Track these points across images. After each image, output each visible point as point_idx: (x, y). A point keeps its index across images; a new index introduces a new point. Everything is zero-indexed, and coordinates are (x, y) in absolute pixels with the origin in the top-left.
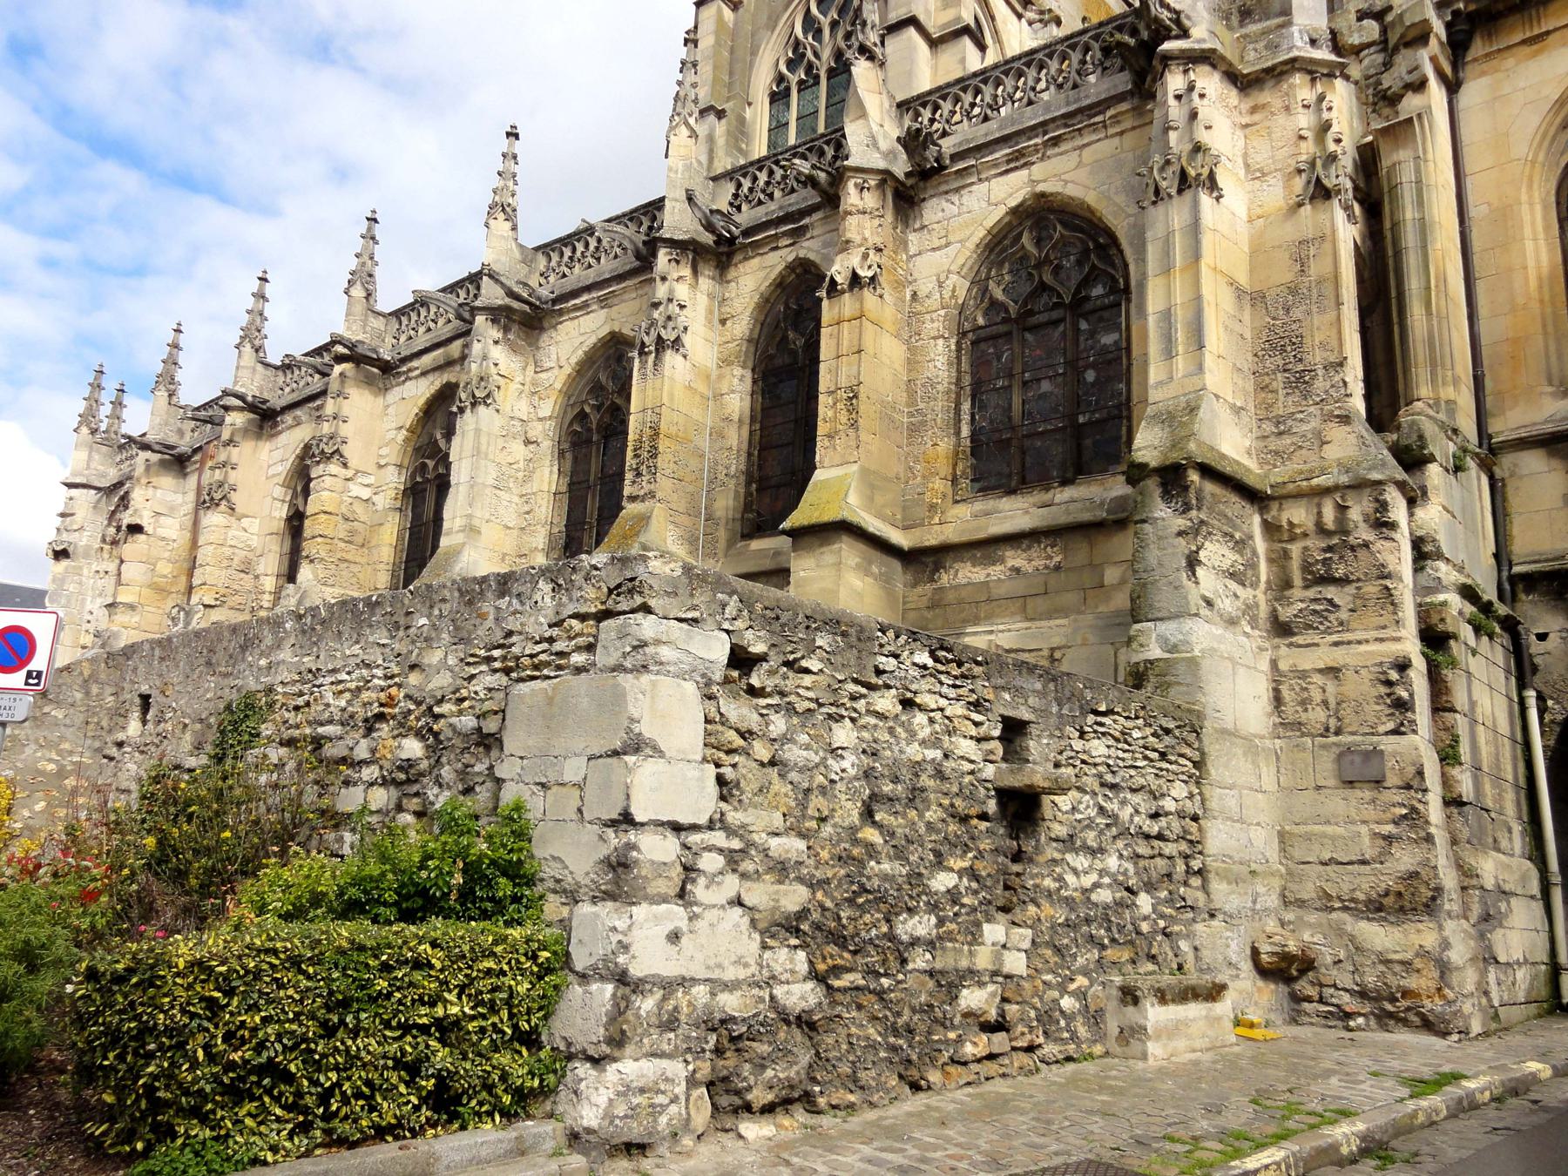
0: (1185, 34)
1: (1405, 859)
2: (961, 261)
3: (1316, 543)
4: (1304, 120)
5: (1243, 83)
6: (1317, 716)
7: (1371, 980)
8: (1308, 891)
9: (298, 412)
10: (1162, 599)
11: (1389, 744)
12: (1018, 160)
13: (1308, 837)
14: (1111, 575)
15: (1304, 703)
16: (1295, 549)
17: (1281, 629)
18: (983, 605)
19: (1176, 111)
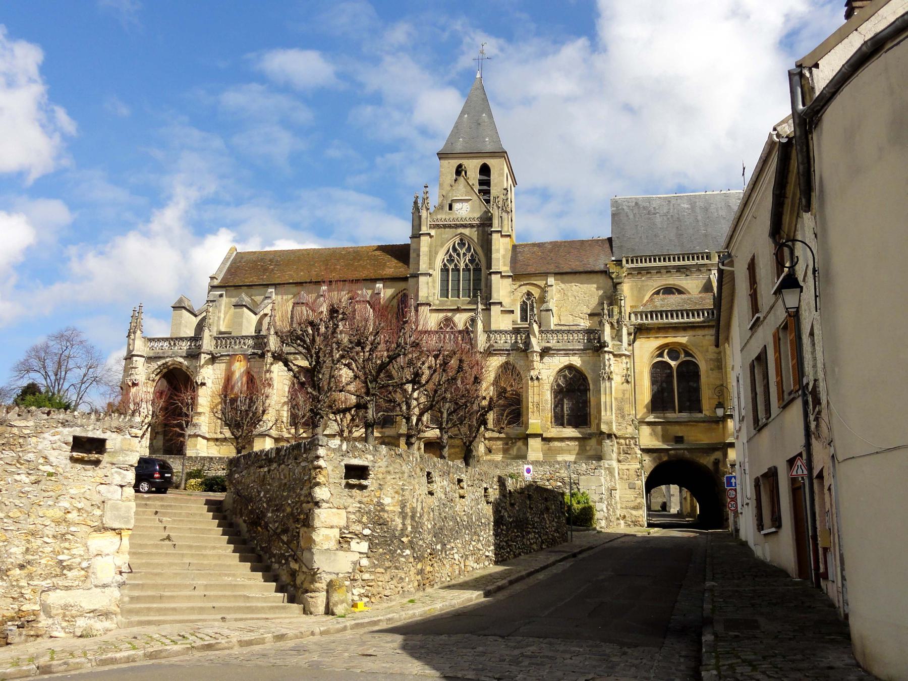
0: (608, 347)
1: (639, 500)
2: (553, 374)
3: (625, 446)
4: (624, 366)
5: (615, 356)
6: (625, 477)
7: (633, 519)
8: (624, 506)
9: (298, 356)
10: (608, 457)
11: (637, 482)
12: (567, 355)
13: (624, 497)
14: (588, 448)
15: (623, 474)
16: (621, 447)
17: (619, 461)
18: (561, 451)
19: (607, 361)
